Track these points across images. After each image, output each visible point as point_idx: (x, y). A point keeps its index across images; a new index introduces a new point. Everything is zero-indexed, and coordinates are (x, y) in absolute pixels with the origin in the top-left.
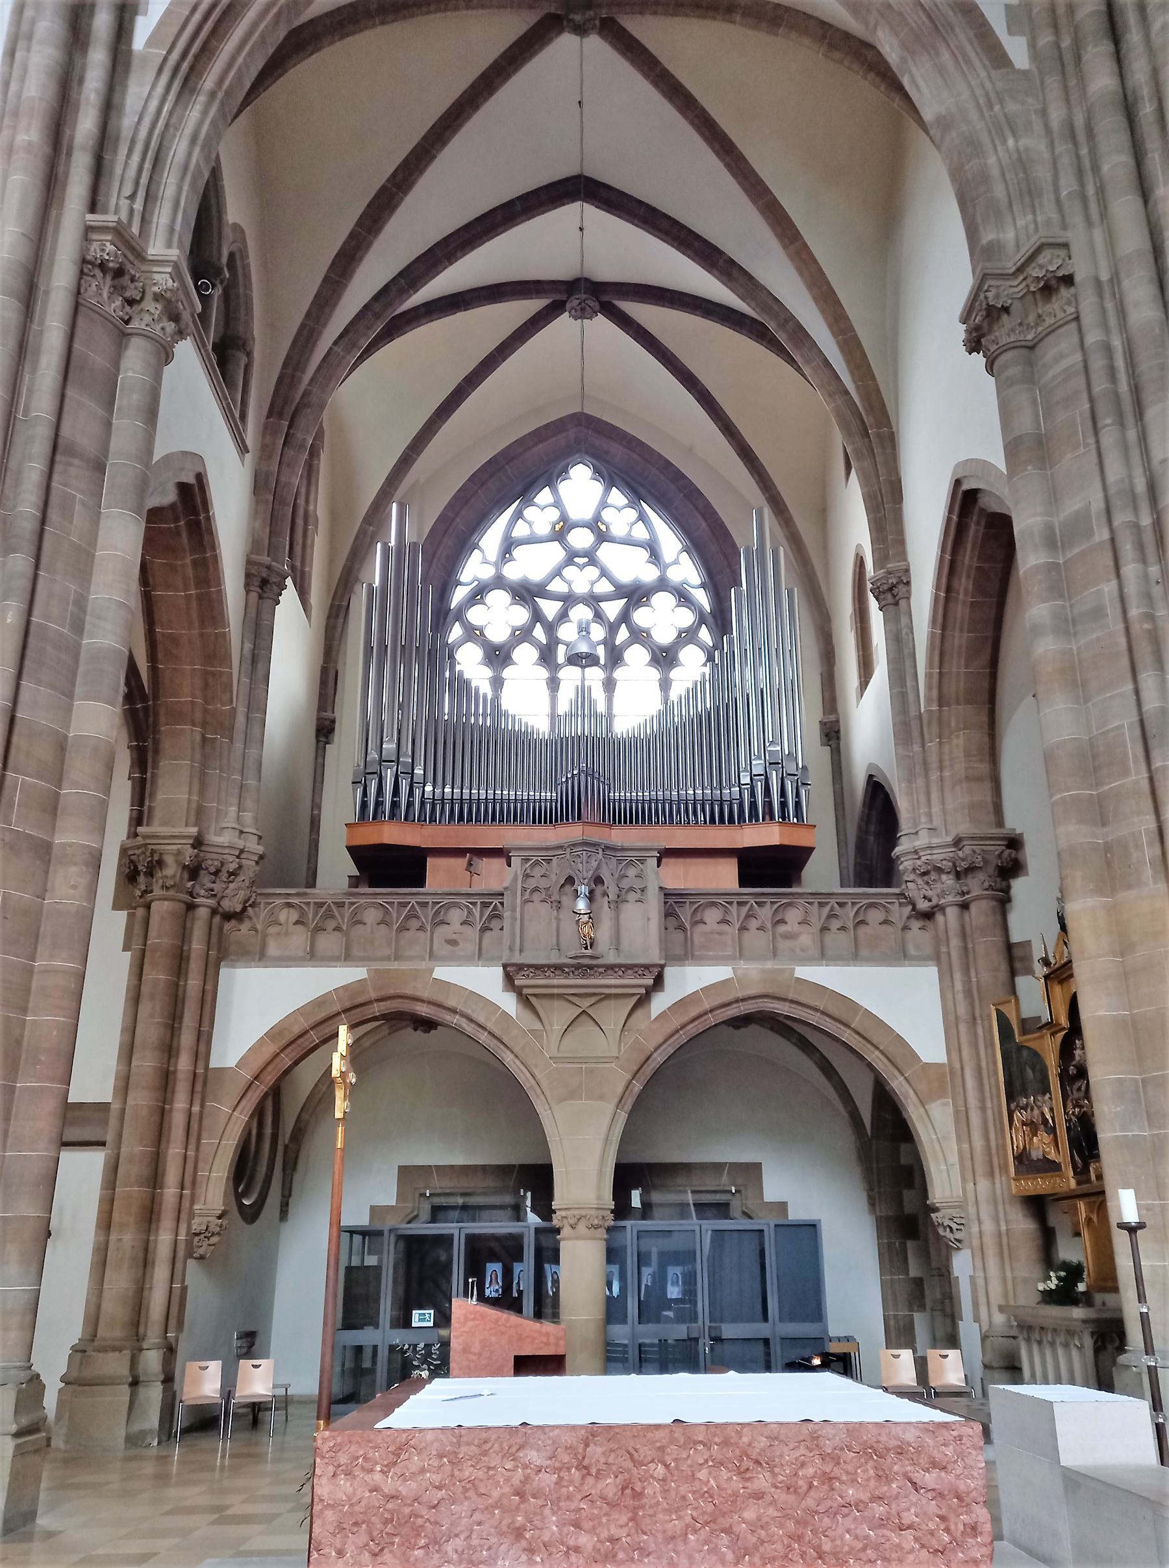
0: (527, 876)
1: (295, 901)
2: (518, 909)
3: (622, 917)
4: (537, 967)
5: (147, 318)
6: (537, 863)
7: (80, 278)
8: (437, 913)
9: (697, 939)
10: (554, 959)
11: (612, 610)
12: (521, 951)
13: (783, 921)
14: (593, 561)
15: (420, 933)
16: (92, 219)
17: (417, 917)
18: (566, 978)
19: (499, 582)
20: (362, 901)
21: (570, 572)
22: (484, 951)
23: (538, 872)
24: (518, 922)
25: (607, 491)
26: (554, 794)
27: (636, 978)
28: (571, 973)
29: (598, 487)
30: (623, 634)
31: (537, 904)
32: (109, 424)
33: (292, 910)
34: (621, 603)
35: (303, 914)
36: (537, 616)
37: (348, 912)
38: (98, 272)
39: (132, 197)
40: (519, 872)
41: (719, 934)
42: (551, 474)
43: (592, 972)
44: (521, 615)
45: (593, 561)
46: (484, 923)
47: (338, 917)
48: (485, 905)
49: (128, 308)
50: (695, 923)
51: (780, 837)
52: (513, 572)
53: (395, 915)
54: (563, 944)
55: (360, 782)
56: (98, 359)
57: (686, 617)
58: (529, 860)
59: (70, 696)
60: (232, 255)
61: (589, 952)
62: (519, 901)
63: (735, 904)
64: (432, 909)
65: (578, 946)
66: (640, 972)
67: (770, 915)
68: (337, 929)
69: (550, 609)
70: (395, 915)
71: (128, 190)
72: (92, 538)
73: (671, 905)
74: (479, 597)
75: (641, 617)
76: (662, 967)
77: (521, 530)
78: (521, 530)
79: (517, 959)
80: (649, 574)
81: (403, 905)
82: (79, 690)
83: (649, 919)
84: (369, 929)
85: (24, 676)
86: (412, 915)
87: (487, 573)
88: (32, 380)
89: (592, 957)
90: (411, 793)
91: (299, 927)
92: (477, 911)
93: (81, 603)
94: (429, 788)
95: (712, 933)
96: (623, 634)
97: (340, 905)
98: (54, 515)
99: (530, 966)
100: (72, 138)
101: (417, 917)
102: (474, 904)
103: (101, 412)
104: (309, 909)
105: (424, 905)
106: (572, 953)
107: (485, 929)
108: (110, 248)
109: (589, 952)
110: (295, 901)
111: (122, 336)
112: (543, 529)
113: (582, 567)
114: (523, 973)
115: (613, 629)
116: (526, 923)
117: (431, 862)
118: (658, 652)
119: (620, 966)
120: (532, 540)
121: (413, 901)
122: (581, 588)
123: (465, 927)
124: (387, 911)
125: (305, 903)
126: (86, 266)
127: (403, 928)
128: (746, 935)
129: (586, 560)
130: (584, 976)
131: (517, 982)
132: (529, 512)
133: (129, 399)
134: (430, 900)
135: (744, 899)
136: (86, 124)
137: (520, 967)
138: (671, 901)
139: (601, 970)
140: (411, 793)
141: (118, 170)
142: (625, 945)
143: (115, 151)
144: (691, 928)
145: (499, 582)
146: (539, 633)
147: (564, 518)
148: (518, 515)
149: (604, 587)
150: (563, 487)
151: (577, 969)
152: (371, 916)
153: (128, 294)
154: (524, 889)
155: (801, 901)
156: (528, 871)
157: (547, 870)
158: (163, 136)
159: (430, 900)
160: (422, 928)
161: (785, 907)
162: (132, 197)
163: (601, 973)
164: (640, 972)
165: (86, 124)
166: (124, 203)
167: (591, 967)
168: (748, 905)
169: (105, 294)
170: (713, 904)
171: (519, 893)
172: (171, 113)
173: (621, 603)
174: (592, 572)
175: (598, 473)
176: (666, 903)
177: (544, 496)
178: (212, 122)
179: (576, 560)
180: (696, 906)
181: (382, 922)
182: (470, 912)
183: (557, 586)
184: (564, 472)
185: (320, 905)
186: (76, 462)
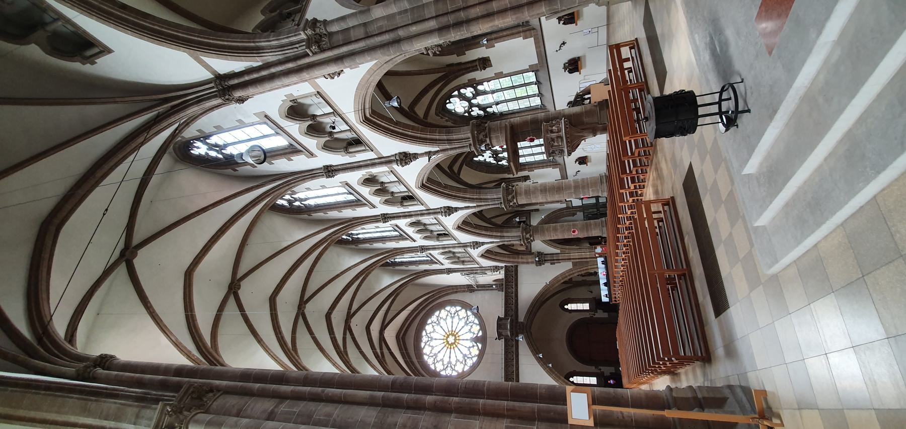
5: (321, 31)
7: (326, 50)
16: (311, 54)
32: (353, 27)
38: (321, 46)
39: (297, 48)
49: (323, 36)
56: (340, 37)
59: (424, 4)
60: (271, 12)
71: (296, 50)
72: (383, 18)
82: (421, 4)
85: (424, 18)
88: (357, 49)
93: (400, 13)
98: (384, 30)
100: (296, 66)
103: (352, 31)
108: (314, 47)
111: (331, 34)
126: (323, 50)
133: (343, 25)
136: (290, 65)
141: (293, 54)
143: (290, 56)
153: (319, 38)
158: (275, 48)
162: (297, 48)
165: (290, 65)
166: (300, 49)
169: (324, 43)
172: (269, 49)
178: (260, 39)
186: (368, 30)
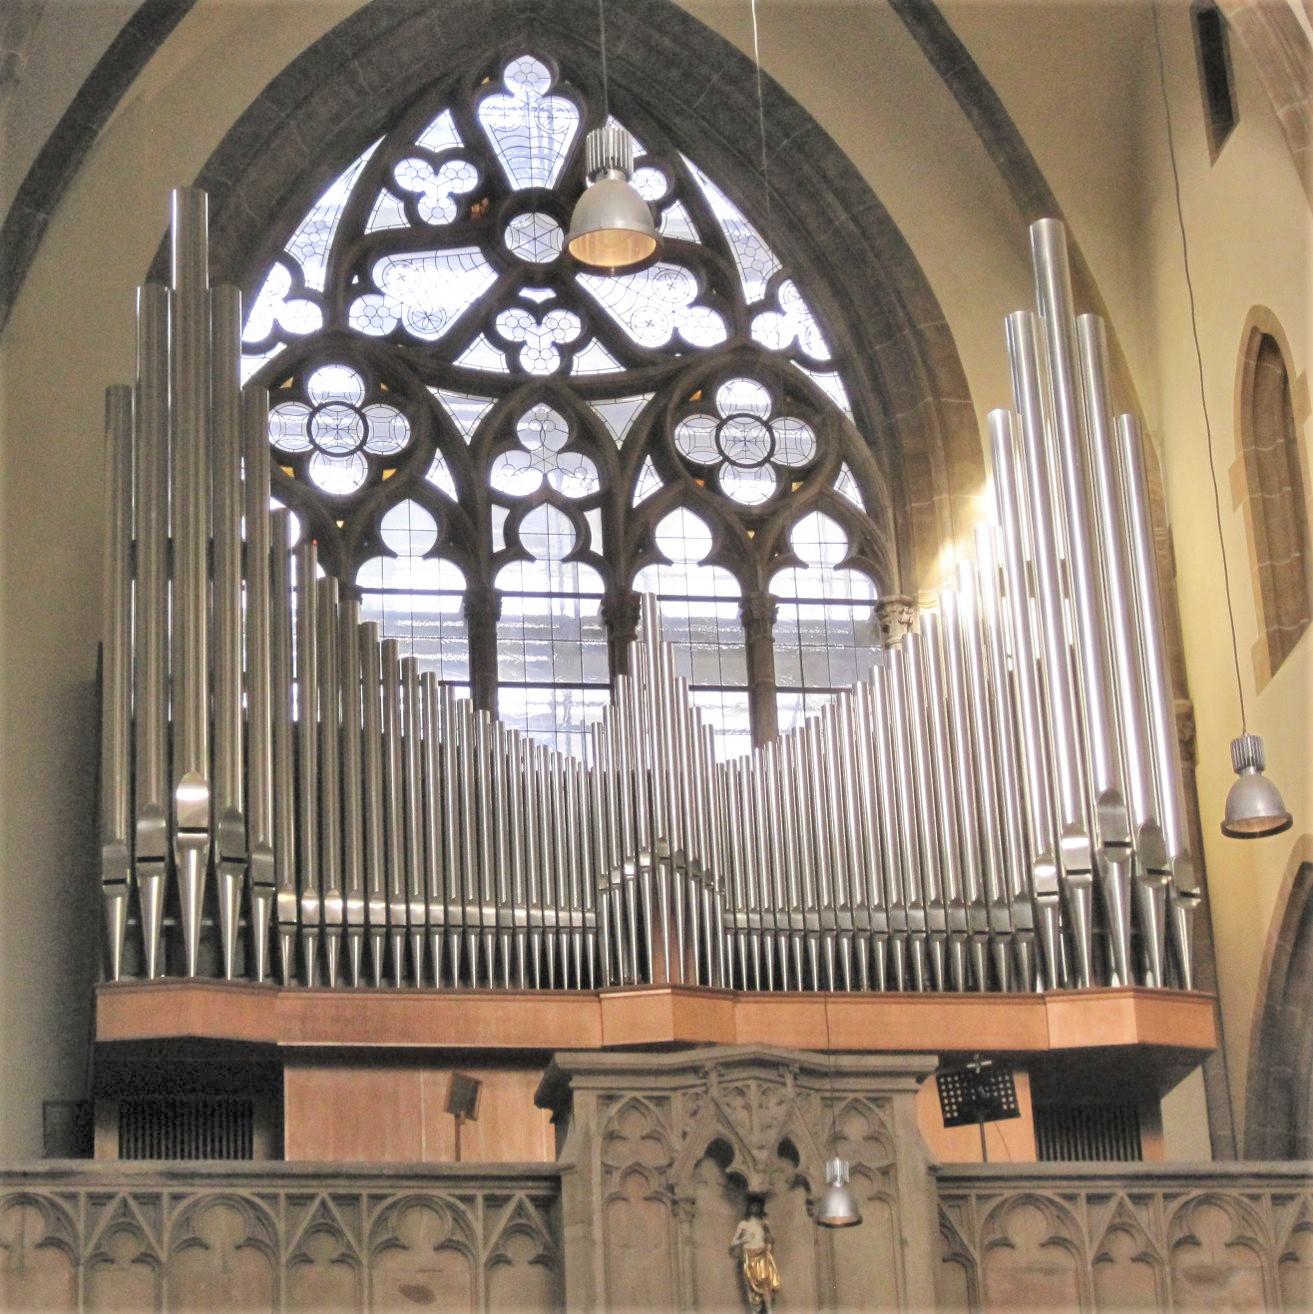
1: (43, 1190)
11: (619, 416)
13: (1191, 1241)
14: (573, 300)
19: (337, 343)
21: (510, 323)
24: (599, 1251)
25: (591, 122)
26: (590, 916)
29: (566, 117)
30: (648, 484)
33: (31, 1213)
34: (636, 404)
35: (62, 1218)
36: (435, 431)
37: (171, 1215)
42: (458, 81)
44: (392, 431)
45: (573, 300)
47: (147, 1229)
51: (1140, 1026)
52: (367, 318)
53: (281, 1227)
55: (123, 881)
57: (798, 442)
62: (596, 1199)
63: (1082, 1201)
68: (146, 1258)
69: (467, 414)
74: (289, 383)
75: (692, 438)
77: (387, 214)
78: (387, 214)
80: (707, 331)
83: (903, 1243)
84: (217, 1261)
87: (307, 320)
90: (246, 911)
91: (51, 1254)
95: (1029, 1269)
96: (648, 484)
97: (151, 1200)
101: (333, 1231)
104: (76, 1207)
110: (43, 1190)
112: (438, 210)
113: (538, 312)
115: (617, 470)
117: (291, 1077)
118: (738, 526)
120: (418, 238)
121: (323, 1193)
122: (540, 363)
124: (262, 1218)
125: (63, 1195)
128: (1108, 1271)
129: (547, 295)
132: (409, 173)
134: (364, 1190)
140: (246, 911)
144: (982, 1262)
145: (337, 343)
146: (441, 477)
147: (493, 182)
148: (379, 178)
149: (595, 361)
150: (492, 113)
152: (222, 1227)
159: (364, 1190)
160: (346, 1259)
170: (1029, 1200)
173: (636, 404)
174: (566, 325)
175: (570, 82)
177: (441, 133)
179: (525, 293)
181: (251, 1242)
183: (481, 357)
184: (491, 79)
185: (98, 1200)
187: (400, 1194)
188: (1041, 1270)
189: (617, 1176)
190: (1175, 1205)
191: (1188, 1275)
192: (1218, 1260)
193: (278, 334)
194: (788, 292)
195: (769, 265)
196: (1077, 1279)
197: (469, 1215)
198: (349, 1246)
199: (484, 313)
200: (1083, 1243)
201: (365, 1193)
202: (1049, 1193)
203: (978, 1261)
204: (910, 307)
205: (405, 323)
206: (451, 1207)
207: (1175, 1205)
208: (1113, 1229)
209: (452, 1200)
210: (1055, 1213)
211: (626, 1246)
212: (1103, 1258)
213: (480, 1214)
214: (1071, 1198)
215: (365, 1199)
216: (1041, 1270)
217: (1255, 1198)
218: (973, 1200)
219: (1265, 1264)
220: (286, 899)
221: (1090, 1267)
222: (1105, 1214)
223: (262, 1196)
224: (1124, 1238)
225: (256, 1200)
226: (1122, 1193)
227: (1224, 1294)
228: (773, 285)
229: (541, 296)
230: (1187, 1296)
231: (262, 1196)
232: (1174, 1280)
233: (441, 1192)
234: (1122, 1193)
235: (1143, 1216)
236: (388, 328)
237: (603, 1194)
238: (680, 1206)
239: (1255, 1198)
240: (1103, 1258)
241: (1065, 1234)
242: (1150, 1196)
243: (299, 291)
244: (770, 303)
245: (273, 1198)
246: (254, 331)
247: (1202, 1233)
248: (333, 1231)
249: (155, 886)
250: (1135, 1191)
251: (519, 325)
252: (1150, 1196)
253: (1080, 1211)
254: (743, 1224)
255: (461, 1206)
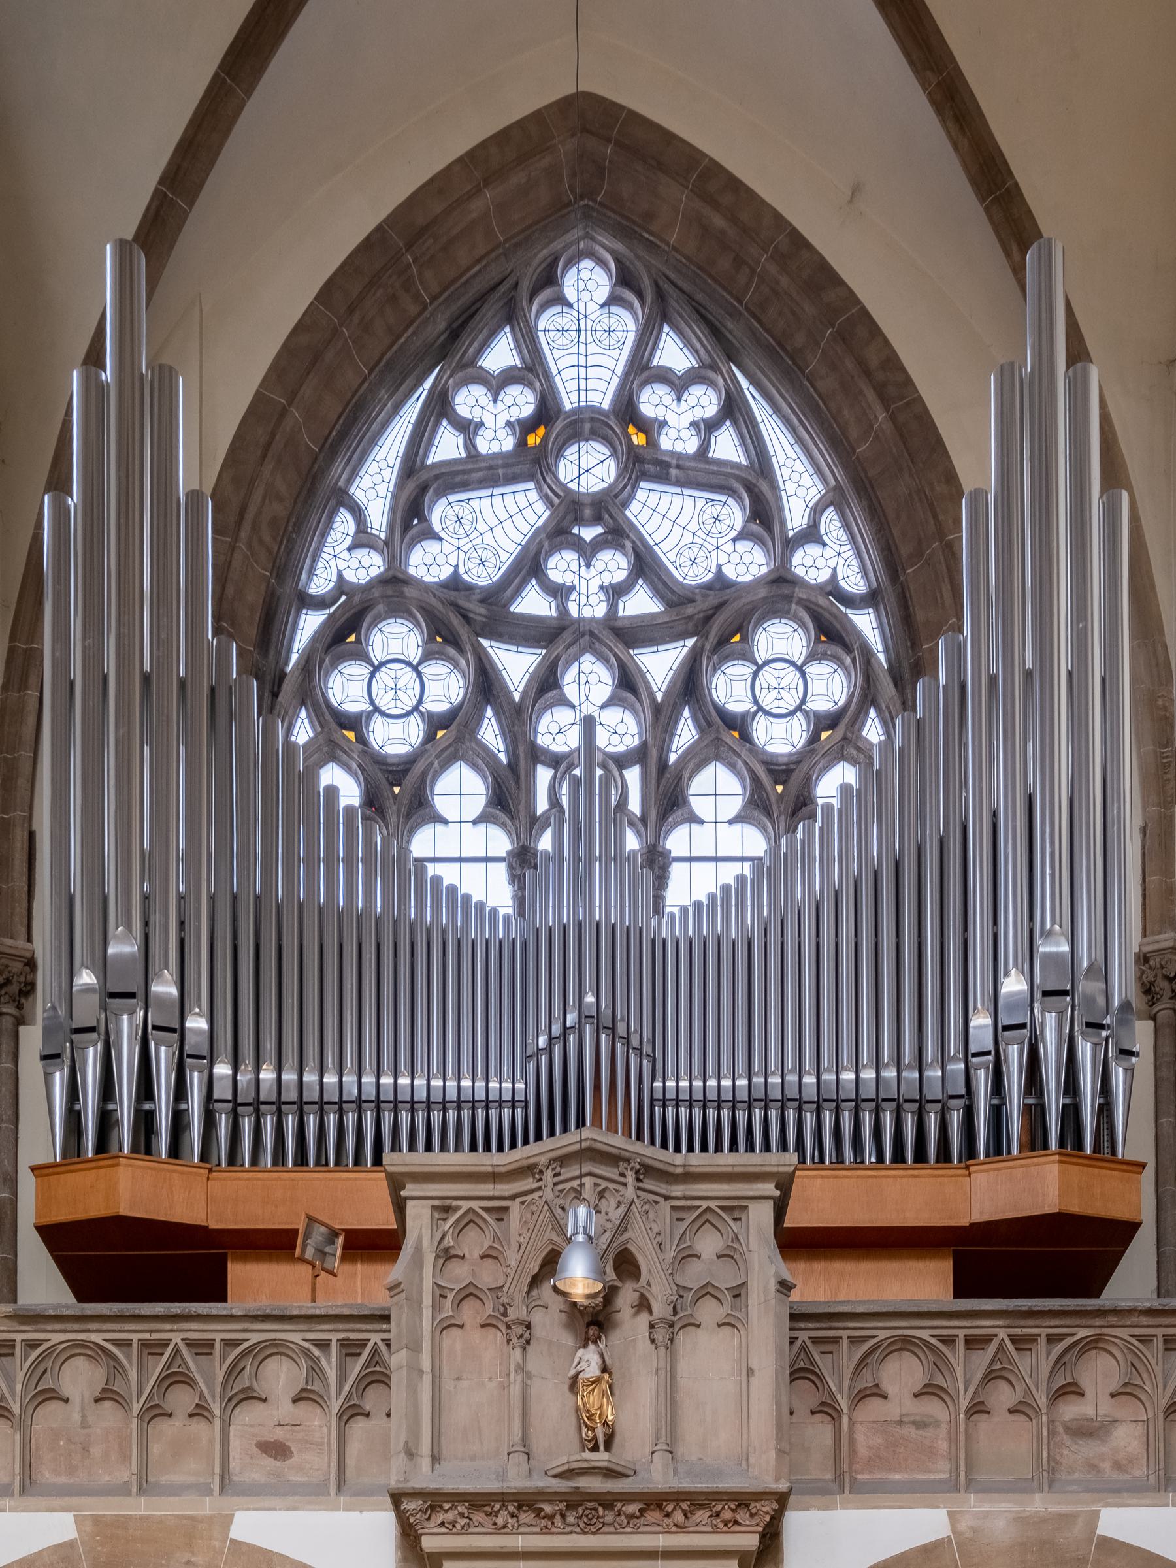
0: (446, 1255)
2: (426, 1345)
3: (683, 1368)
4: (478, 1502)
6: (470, 1220)
8: (234, 1371)
9: (865, 1441)
10: (517, 1480)
12: (435, 1459)
13: (1072, 1390)
15: (199, 1427)
17: (189, 1382)
18: (545, 1531)
20: (56, 1338)
22: (350, 1472)
23: (473, 1243)
27: (715, 1531)
28: (558, 1520)
31: (476, 1336)
40: (426, 1243)
41: (920, 1425)
43: (610, 1517)
46: (349, 1396)
48: (350, 1349)
50: (862, 1396)
53: (133, 1374)
54: (537, 1447)
58: (447, 1210)
61: (601, 1458)
63: (961, 1344)
64: (223, 1358)
65: (576, 1445)
66: (727, 1515)
67: (1046, 1370)
70: (133, 1374)
73: (803, 1348)
76: (782, 1500)
79: (425, 1477)
81: (152, 1348)
86: (175, 1378)
89: (610, 1473)
92: (330, 1365)
94: (222, 1070)
99: (457, 1498)
101: (189, 1382)
102: (324, 1345)
105: (202, 1347)
106: (560, 1461)
107: (352, 1412)
109: (601, 1458)
113: (588, 552)
114: (441, 1517)
116: (448, 1385)
119: (678, 1497)
121: (177, 1338)
123: (304, 1408)
127: (155, 1412)
130: (590, 1525)
131: (429, 1543)
135: (983, 1326)
137: (435, 1500)
138: (803, 1336)
139: (632, 1508)
142: (689, 1449)
151: (571, 1506)
154: (440, 1293)
155: (1123, 1333)
156: (449, 1241)
157: (496, 1238)
160: (200, 1412)
161: (1082, 1352)
163: (631, 1517)
164: (727, 1515)
167: (607, 1501)
168: (992, 1348)
170: (905, 1344)
171: (427, 1300)
176: (792, 1340)
180: (866, 1347)
182: (315, 1369)
187: (255, 1338)
188: (914, 1423)
189: (448, 1303)
190: (1059, 1348)
191: (1067, 1429)
192: (1101, 1412)
193: (342, 585)
194: (830, 522)
195: (814, 491)
196: (950, 1432)
197: (323, 1361)
198: (202, 1396)
199: (532, 554)
200: (957, 1389)
201: (218, 1337)
202: (924, 1334)
203: (846, 1410)
204: (941, 517)
205: (461, 570)
206: (307, 1353)
207: (1059, 1348)
208: (990, 1377)
209: (306, 1345)
210: (932, 1358)
211: (458, 1379)
212: (977, 1409)
213: (334, 1359)
214: (949, 1341)
215: (218, 1345)
216: (914, 1423)
217: (1145, 1340)
218: (845, 1343)
219: (1151, 1415)
220: (222, 1070)
221: (962, 1416)
222: (982, 1359)
223: (114, 1342)
224: (1003, 1386)
225: (108, 1346)
226: (1002, 1334)
227: (1104, 1449)
228: (817, 511)
229: (588, 533)
230: (1065, 1452)
231: (114, 1342)
232: (1052, 1433)
233: (295, 1337)
234: (1002, 1334)
235: (1024, 1363)
236: (446, 573)
237: (433, 1319)
238: (524, 1335)
239: (1145, 1340)
240: (977, 1409)
241: (940, 1381)
242: (1033, 1339)
243: (362, 539)
244: (811, 534)
245: (125, 1344)
246: (320, 584)
247: (1085, 1383)
248: (187, 1380)
249: (92, 1057)
250: (1017, 1331)
251: (569, 569)
252: (1033, 1339)
253: (957, 1356)
254: (580, 1352)
255: (316, 1352)
